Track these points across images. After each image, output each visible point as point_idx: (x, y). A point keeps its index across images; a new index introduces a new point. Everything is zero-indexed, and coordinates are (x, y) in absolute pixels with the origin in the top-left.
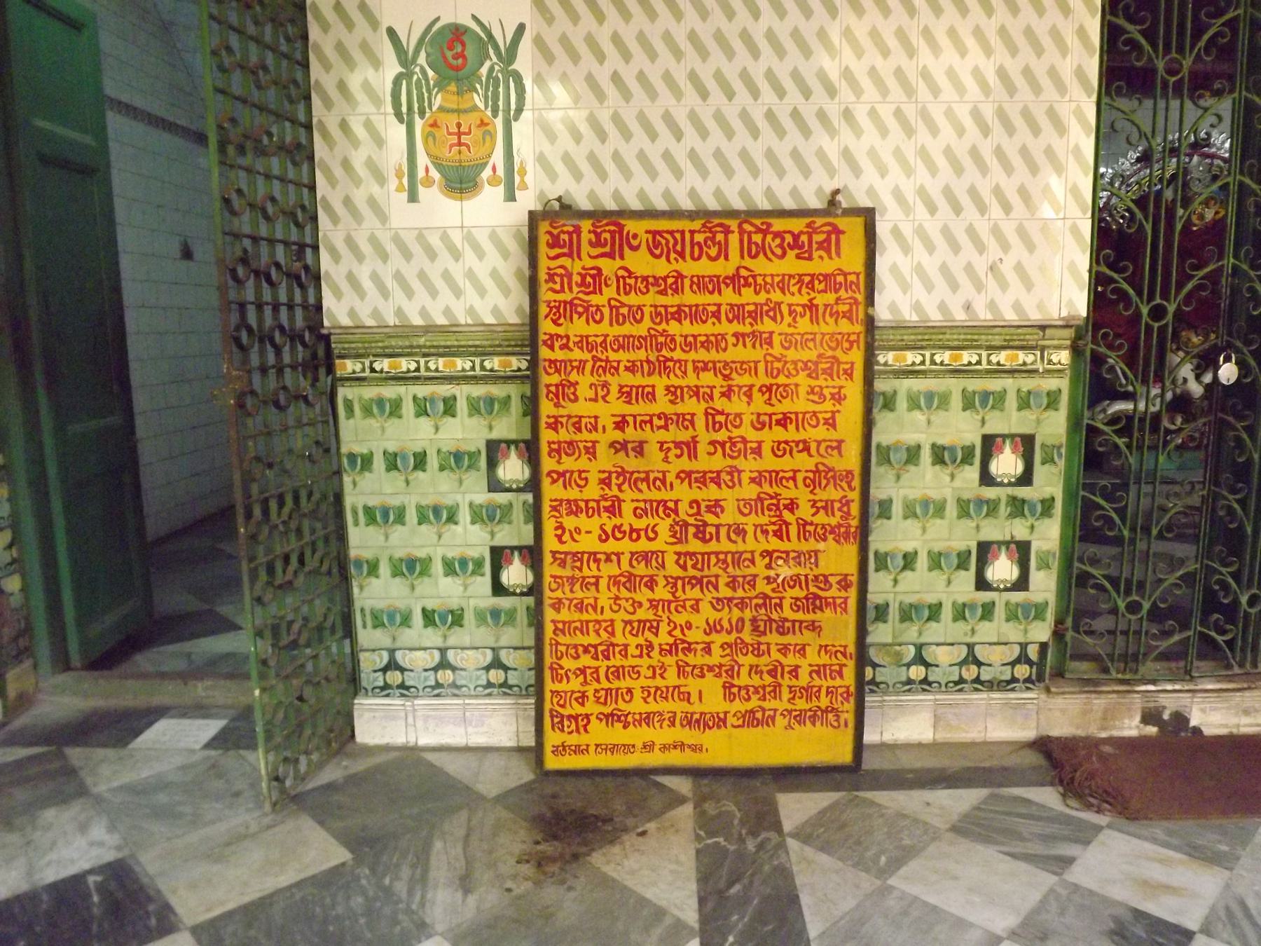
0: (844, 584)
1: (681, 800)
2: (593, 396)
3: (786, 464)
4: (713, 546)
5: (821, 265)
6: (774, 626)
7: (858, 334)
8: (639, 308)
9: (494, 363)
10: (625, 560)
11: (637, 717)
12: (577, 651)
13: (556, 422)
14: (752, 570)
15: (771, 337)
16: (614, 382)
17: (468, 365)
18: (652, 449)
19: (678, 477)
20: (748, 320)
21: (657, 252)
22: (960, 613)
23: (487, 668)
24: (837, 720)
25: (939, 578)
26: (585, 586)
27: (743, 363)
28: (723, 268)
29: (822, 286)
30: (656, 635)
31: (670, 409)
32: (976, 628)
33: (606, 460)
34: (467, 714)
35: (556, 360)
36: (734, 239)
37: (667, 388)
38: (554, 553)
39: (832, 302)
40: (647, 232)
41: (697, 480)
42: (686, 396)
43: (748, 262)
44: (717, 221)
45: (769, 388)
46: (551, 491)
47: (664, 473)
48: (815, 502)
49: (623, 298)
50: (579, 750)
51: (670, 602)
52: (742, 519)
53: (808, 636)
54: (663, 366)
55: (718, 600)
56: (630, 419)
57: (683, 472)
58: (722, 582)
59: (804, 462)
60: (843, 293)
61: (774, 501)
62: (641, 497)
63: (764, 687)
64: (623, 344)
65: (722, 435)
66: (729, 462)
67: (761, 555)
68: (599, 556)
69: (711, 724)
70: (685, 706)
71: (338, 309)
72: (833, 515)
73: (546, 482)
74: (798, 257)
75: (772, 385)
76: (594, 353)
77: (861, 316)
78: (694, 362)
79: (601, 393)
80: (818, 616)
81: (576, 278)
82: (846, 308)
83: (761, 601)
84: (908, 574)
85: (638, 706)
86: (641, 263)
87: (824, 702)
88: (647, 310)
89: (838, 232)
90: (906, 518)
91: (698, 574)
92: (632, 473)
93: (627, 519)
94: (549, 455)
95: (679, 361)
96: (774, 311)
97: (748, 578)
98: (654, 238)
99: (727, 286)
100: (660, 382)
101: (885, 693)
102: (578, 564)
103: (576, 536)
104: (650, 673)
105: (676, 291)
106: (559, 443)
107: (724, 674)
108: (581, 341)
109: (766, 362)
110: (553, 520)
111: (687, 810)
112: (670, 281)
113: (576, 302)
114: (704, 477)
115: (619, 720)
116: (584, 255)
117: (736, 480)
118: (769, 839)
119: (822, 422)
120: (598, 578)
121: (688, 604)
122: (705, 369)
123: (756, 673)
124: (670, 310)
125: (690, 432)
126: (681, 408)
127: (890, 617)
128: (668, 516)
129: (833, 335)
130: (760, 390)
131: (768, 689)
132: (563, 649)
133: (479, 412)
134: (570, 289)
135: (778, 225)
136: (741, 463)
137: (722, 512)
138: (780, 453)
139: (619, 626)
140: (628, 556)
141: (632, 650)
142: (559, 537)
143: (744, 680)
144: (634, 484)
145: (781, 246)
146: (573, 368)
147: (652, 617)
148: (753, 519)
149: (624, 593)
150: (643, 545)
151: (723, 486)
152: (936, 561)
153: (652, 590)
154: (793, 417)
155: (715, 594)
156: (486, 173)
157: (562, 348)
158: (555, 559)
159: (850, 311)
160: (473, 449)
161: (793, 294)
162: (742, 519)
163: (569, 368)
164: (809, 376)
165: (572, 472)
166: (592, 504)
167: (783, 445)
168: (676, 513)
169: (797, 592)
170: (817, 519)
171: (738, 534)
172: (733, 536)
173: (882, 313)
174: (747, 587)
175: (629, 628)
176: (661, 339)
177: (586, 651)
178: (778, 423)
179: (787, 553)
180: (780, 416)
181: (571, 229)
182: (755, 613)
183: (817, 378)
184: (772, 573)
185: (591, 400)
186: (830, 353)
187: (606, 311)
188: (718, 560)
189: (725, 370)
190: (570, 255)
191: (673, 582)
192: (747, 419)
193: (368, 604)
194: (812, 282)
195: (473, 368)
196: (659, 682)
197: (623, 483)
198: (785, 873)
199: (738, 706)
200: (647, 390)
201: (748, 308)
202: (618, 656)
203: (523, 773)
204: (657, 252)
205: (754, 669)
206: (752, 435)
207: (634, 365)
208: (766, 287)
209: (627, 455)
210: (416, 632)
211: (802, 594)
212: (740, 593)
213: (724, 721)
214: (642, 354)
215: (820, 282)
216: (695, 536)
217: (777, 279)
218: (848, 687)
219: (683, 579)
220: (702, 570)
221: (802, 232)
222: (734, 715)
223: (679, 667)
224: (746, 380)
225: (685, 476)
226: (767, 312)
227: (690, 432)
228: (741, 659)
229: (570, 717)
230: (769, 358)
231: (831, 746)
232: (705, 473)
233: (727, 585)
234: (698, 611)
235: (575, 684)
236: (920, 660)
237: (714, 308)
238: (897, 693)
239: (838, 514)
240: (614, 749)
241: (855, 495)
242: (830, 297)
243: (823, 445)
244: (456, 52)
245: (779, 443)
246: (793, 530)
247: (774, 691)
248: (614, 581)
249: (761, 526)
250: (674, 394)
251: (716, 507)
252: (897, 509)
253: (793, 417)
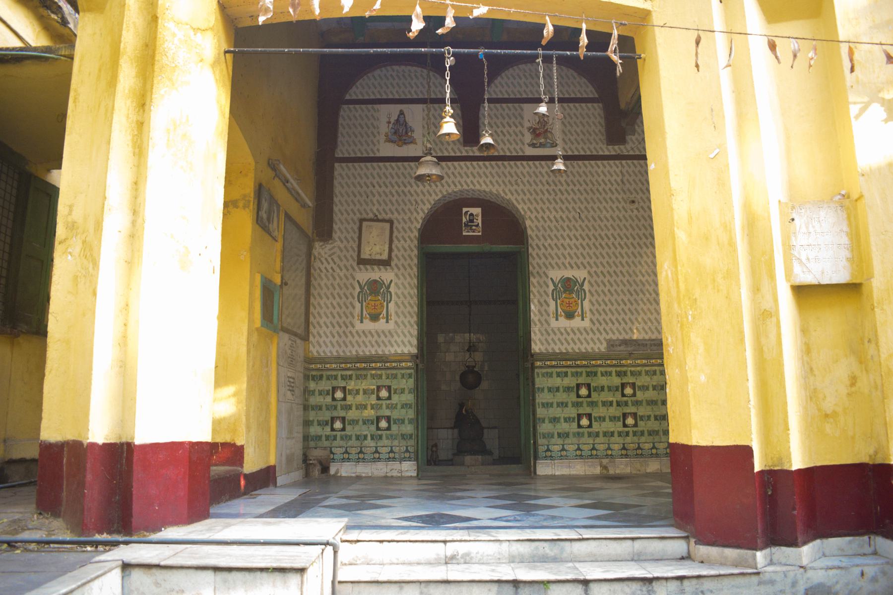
71: (536, 347)
193: (541, 431)
210: (556, 440)
244: (568, 285)
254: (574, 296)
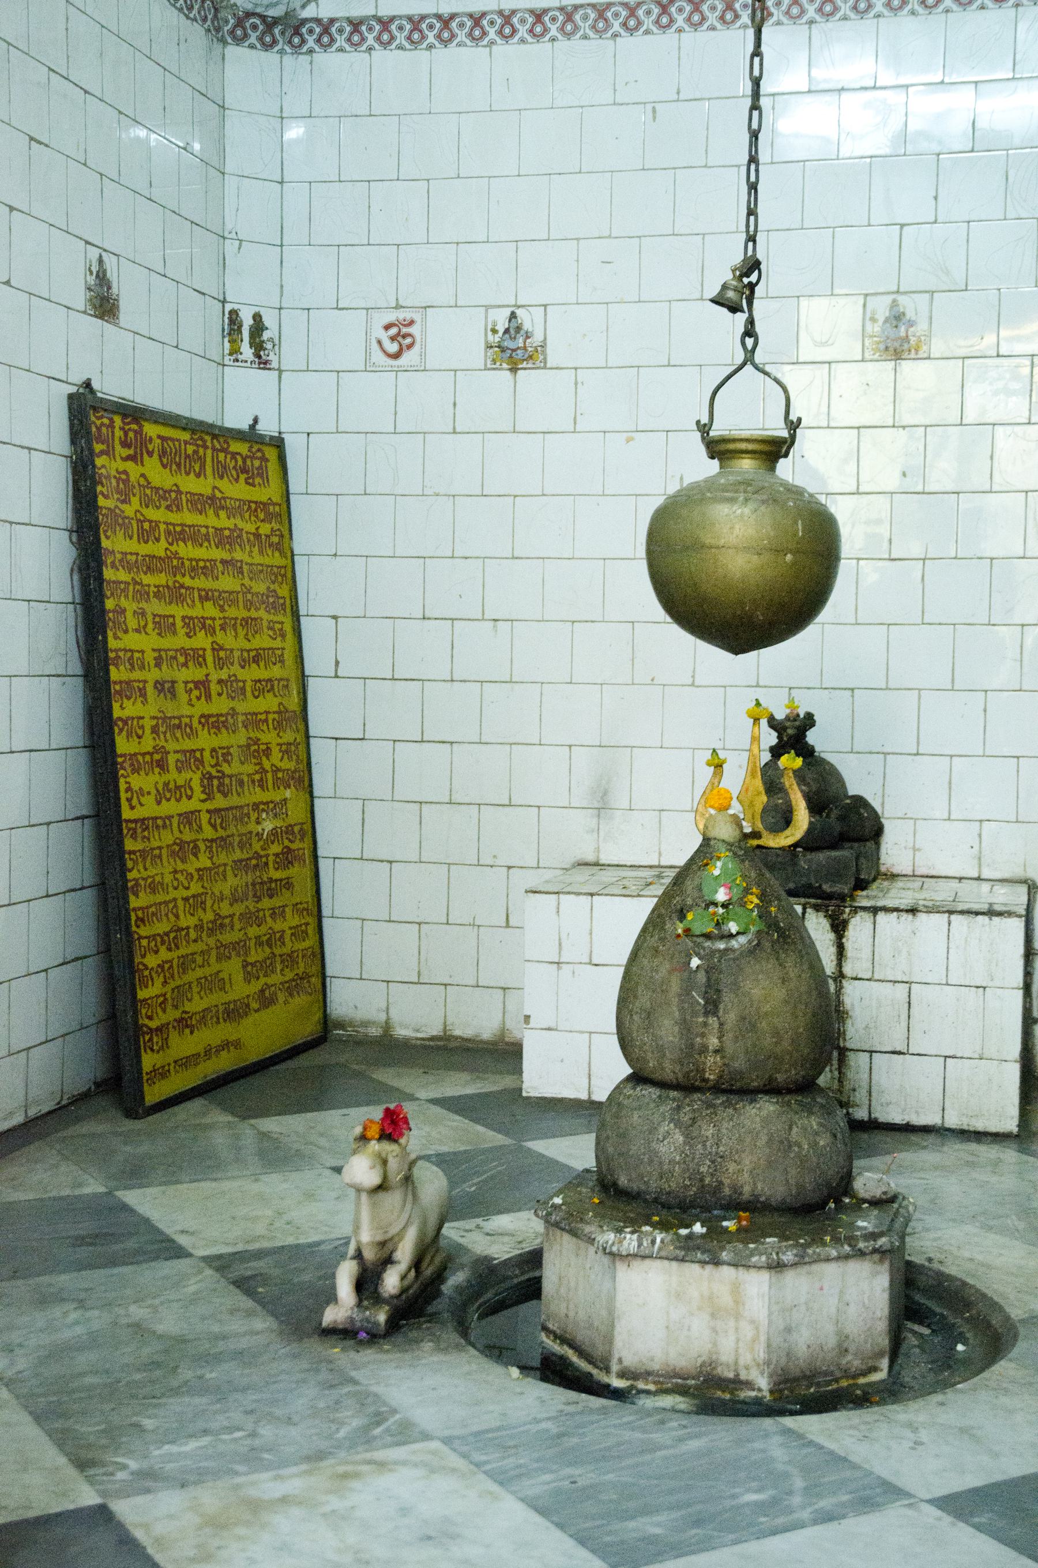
40: (159, 437)
54: (176, 594)
61: (256, 747)
66: (232, 704)
78: (199, 590)
125: (204, 671)
128: (198, 769)
149: (180, 866)
169: (276, 848)
213: (248, 1005)
227: (204, 671)
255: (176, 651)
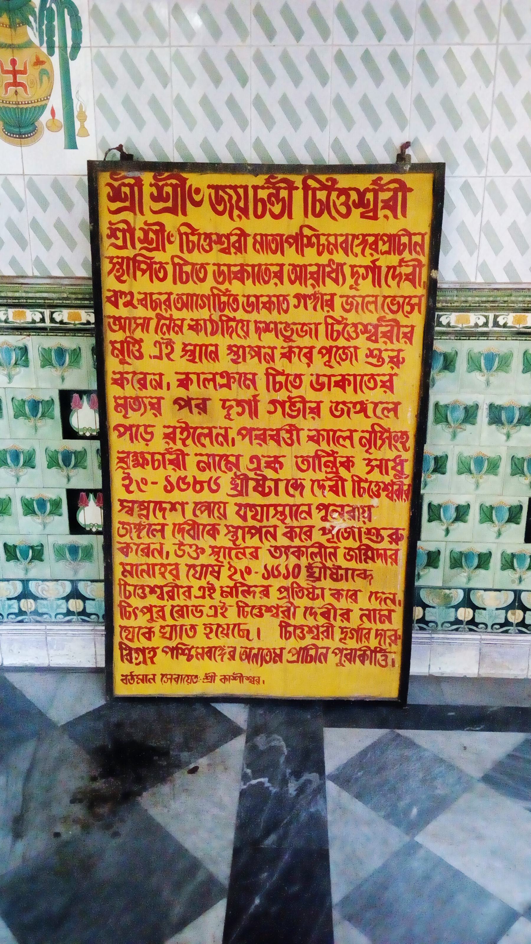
0: (395, 537)
1: (235, 731)
2: (158, 354)
3: (343, 424)
4: (272, 499)
5: (387, 225)
6: (328, 572)
7: (420, 298)
8: (203, 266)
9: (63, 315)
10: (189, 509)
11: (200, 651)
12: (143, 591)
13: (122, 378)
14: (309, 522)
15: (332, 300)
16: (178, 340)
17: (38, 317)
18: (215, 406)
19: (239, 433)
20: (310, 282)
21: (220, 208)
22: (509, 562)
23: (67, 598)
24: (386, 660)
25: (489, 530)
26: (151, 532)
27: (304, 325)
28: (286, 227)
29: (386, 248)
30: (218, 578)
31: (232, 368)
32: (523, 577)
33: (170, 416)
34: (49, 638)
35: (120, 318)
36: (298, 196)
37: (230, 347)
38: (122, 502)
39: (396, 263)
40: (209, 187)
41: (257, 437)
42: (248, 356)
43: (312, 221)
44: (280, 176)
45: (329, 350)
46: (118, 444)
47: (226, 429)
48: (370, 460)
49: (187, 256)
50: (145, 679)
51: (230, 549)
52: (300, 475)
53: (359, 583)
54: (224, 326)
55: (276, 548)
56: (194, 377)
57: (244, 428)
58: (281, 531)
59: (360, 423)
60: (406, 255)
61: (332, 459)
62: (204, 451)
63: (317, 628)
64: (188, 302)
65: (282, 395)
66: (289, 421)
67: (317, 508)
68: (164, 505)
69: (268, 658)
70: (244, 642)
72: (387, 473)
73: (113, 436)
74: (363, 216)
75: (331, 347)
76: (158, 311)
77: (424, 278)
78: (256, 322)
79: (165, 351)
80: (370, 566)
81: (139, 234)
82: (409, 270)
83: (316, 550)
84: (460, 524)
85: (200, 641)
86: (203, 218)
87: (373, 643)
88: (210, 269)
89: (404, 189)
90: (460, 473)
91: (258, 525)
92: (196, 429)
93: (191, 471)
94: (116, 410)
95: (242, 321)
96: (336, 272)
97: (305, 529)
98: (217, 193)
99: (291, 245)
100: (222, 342)
101: (435, 631)
102: (145, 512)
103: (142, 486)
104: (212, 612)
105: (239, 250)
106: (125, 398)
107: (281, 615)
108: (145, 299)
109: (327, 324)
110: (121, 470)
111: (238, 744)
112: (233, 239)
113: (139, 258)
114: (264, 434)
115: (183, 654)
116: (146, 209)
117: (295, 437)
118: (309, 781)
119: (380, 384)
120: (163, 525)
121: (248, 551)
122: (267, 329)
123: (311, 614)
124: (233, 269)
126: (242, 368)
127: (441, 563)
128: (230, 470)
129: (394, 297)
130: (320, 352)
131: (321, 629)
132: (131, 589)
133: (51, 364)
134: (134, 247)
135: (344, 181)
136: (299, 422)
137: (281, 468)
138: (338, 414)
139: (183, 570)
140: (191, 506)
141: (195, 592)
142: (127, 488)
143: (299, 620)
144: (198, 439)
145: (345, 204)
146: (138, 325)
147: (216, 563)
148: (310, 475)
149: (188, 540)
150: (206, 496)
151: (282, 442)
152: (488, 514)
153: (215, 539)
154: (351, 378)
155: (274, 543)
156: (45, 117)
157: (126, 305)
158: (123, 507)
159: (413, 273)
160: (47, 398)
161: (356, 255)
162: (300, 475)
163: (134, 326)
164: (368, 339)
165: (138, 426)
166: (157, 457)
167: (341, 406)
168: (238, 468)
169: (351, 543)
170: (370, 477)
171: (296, 489)
172: (291, 491)
173: (447, 275)
174: (303, 537)
175: (192, 572)
176: (224, 299)
177: (152, 591)
178: (337, 384)
179: (342, 507)
180: (339, 378)
181: (132, 181)
182: (310, 561)
183: (376, 341)
184: (327, 525)
185: (155, 357)
186: (390, 316)
187: (170, 268)
188: (277, 512)
189: (285, 332)
190: (131, 209)
191: (233, 531)
192: (306, 381)
194: (376, 243)
195: (43, 320)
196: (220, 620)
197: (187, 437)
198: (318, 824)
199: (293, 643)
200: (210, 348)
201: (310, 269)
202: (182, 597)
203: (95, 700)
204: (220, 208)
205: (309, 611)
206: (311, 395)
207: (197, 324)
208: (331, 248)
209: (191, 412)
211: (357, 545)
212: (297, 542)
213: (280, 656)
214: (204, 314)
215: (384, 243)
216: (255, 489)
217: (340, 239)
218: (396, 631)
219: (243, 528)
220: (261, 521)
221: (367, 190)
222: (289, 652)
223: (239, 607)
224: (306, 341)
225: (246, 432)
226: (329, 273)
228: (297, 602)
229: (137, 650)
230: (330, 321)
231: (379, 682)
232: (265, 430)
233: (285, 534)
234: (257, 558)
235: (142, 620)
236: (467, 602)
237: (276, 269)
238: (445, 631)
239: (392, 473)
240: (179, 678)
241: (409, 456)
242: (393, 260)
243: (380, 407)
245: (338, 403)
246: (349, 486)
247: (327, 631)
248: (179, 528)
249: (318, 481)
250: (236, 353)
251: (275, 463)
252: (452, 465)
253: (351, 378)
254: (32, 34)
255: (217, 373)
